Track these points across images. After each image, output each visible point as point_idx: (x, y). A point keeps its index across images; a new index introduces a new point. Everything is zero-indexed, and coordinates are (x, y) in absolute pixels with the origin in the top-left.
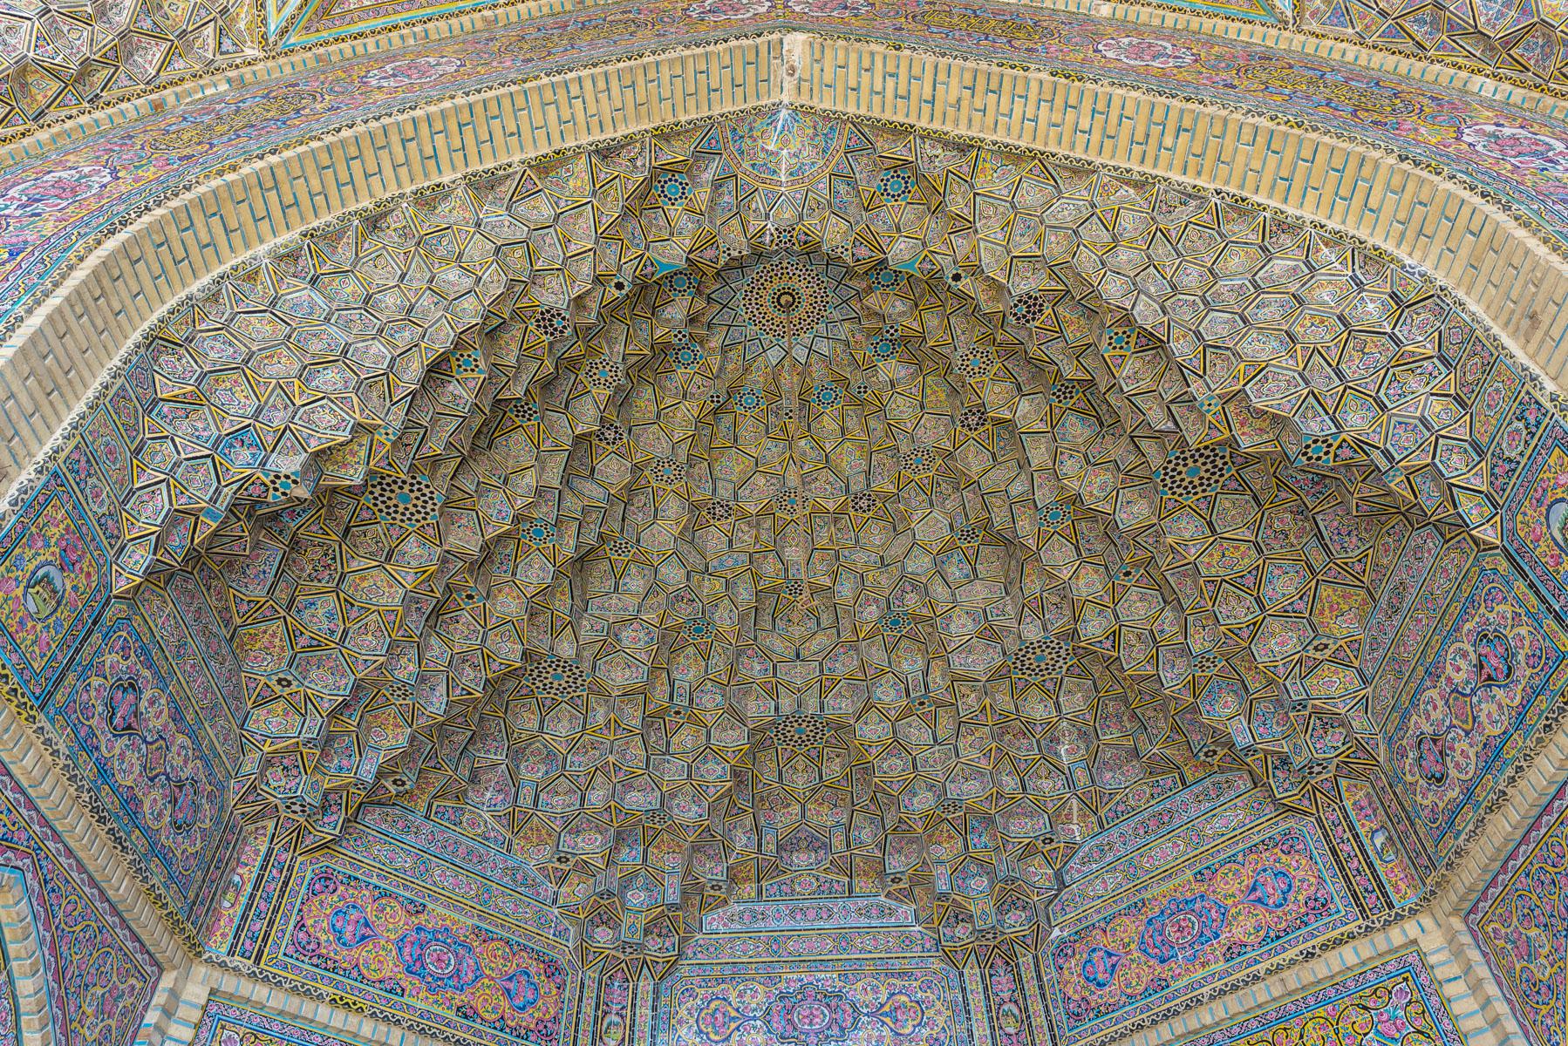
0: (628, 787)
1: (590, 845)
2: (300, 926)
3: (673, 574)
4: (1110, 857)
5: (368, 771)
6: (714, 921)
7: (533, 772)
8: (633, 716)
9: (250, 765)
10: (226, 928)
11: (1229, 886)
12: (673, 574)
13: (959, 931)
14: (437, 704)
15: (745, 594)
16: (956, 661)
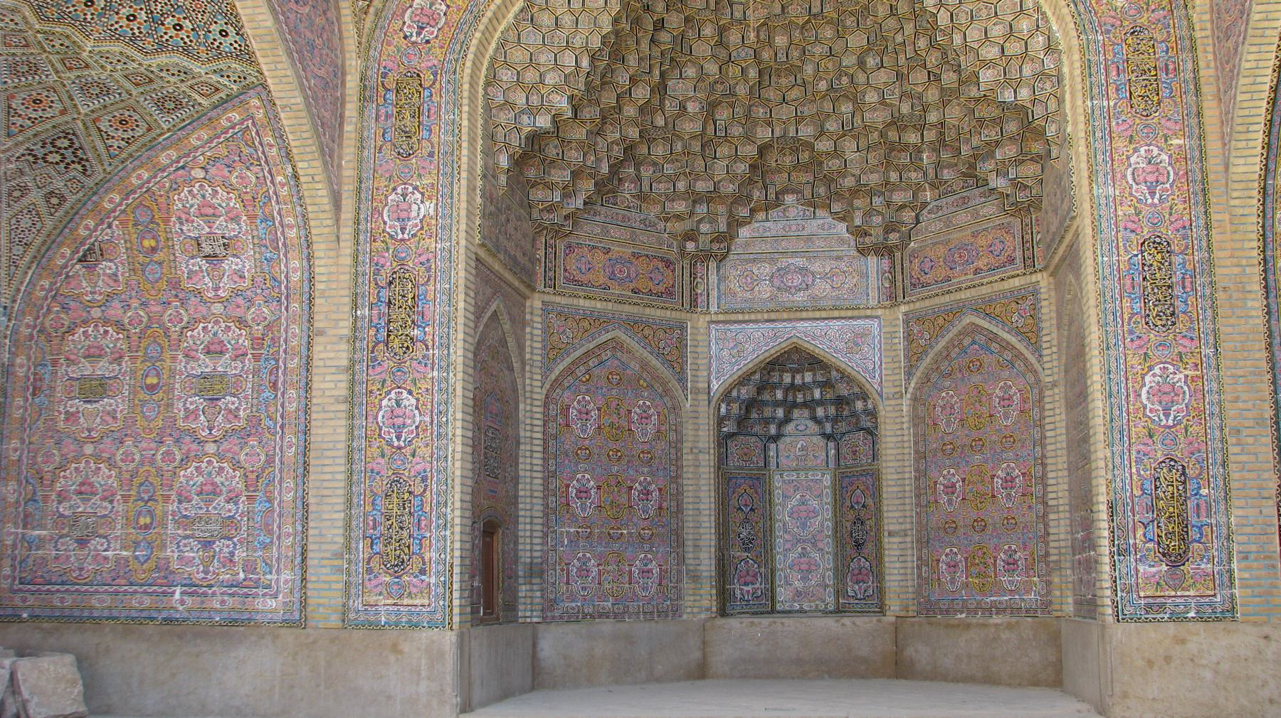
0: (696, 180)
1: (680, 207)
2: (565, 270)
3: (712, 68)
4: (940, 213)
5: (579, 203)
6: (744, 232)
7: (646, 172)
8: (696, 146)
9: (535, 215)
10: (540, 277)
11: (982, 241)
12: (712, 68)
13: (867, 240)
14: (605, 169)
15: (753, 73)
16: (867, 115)
